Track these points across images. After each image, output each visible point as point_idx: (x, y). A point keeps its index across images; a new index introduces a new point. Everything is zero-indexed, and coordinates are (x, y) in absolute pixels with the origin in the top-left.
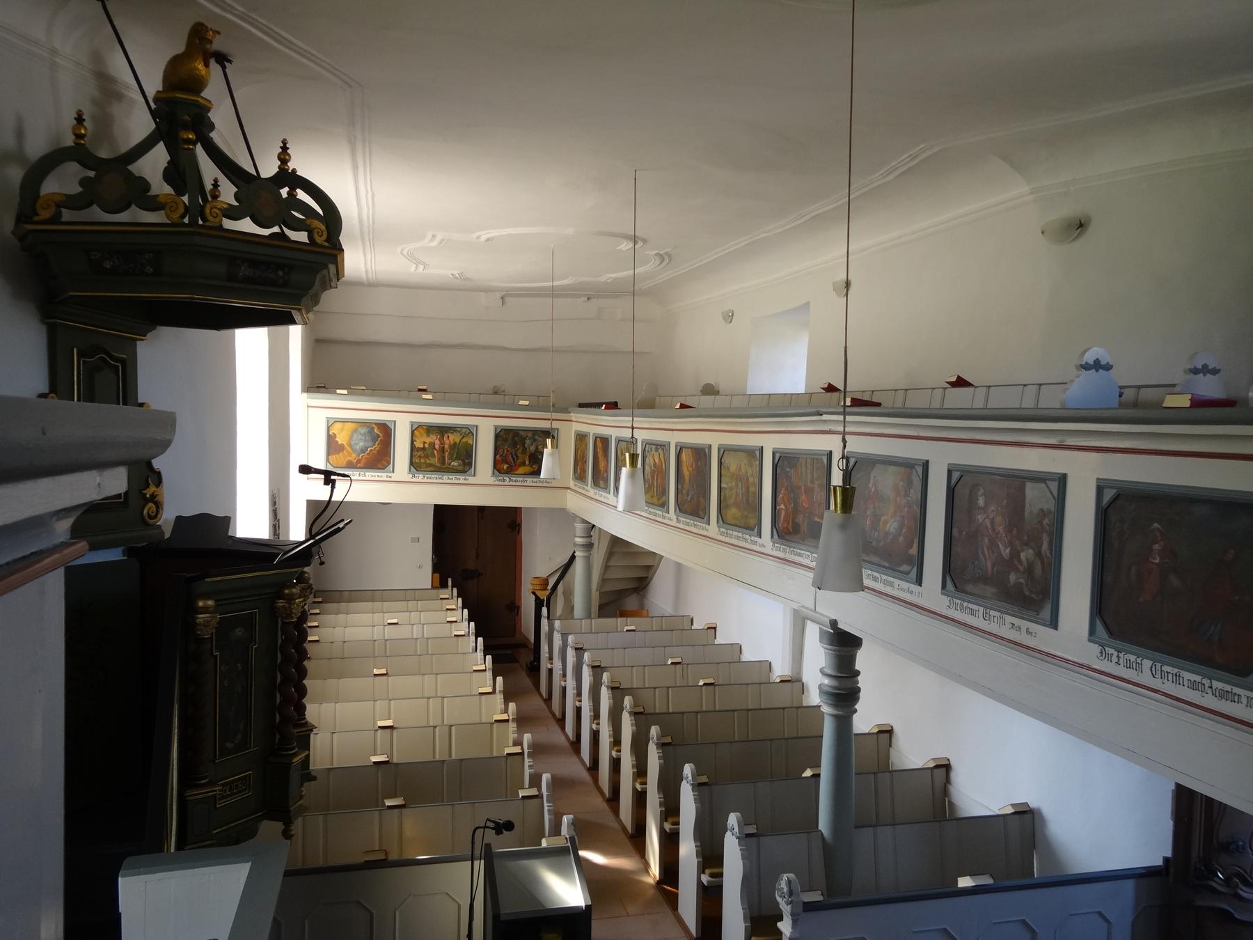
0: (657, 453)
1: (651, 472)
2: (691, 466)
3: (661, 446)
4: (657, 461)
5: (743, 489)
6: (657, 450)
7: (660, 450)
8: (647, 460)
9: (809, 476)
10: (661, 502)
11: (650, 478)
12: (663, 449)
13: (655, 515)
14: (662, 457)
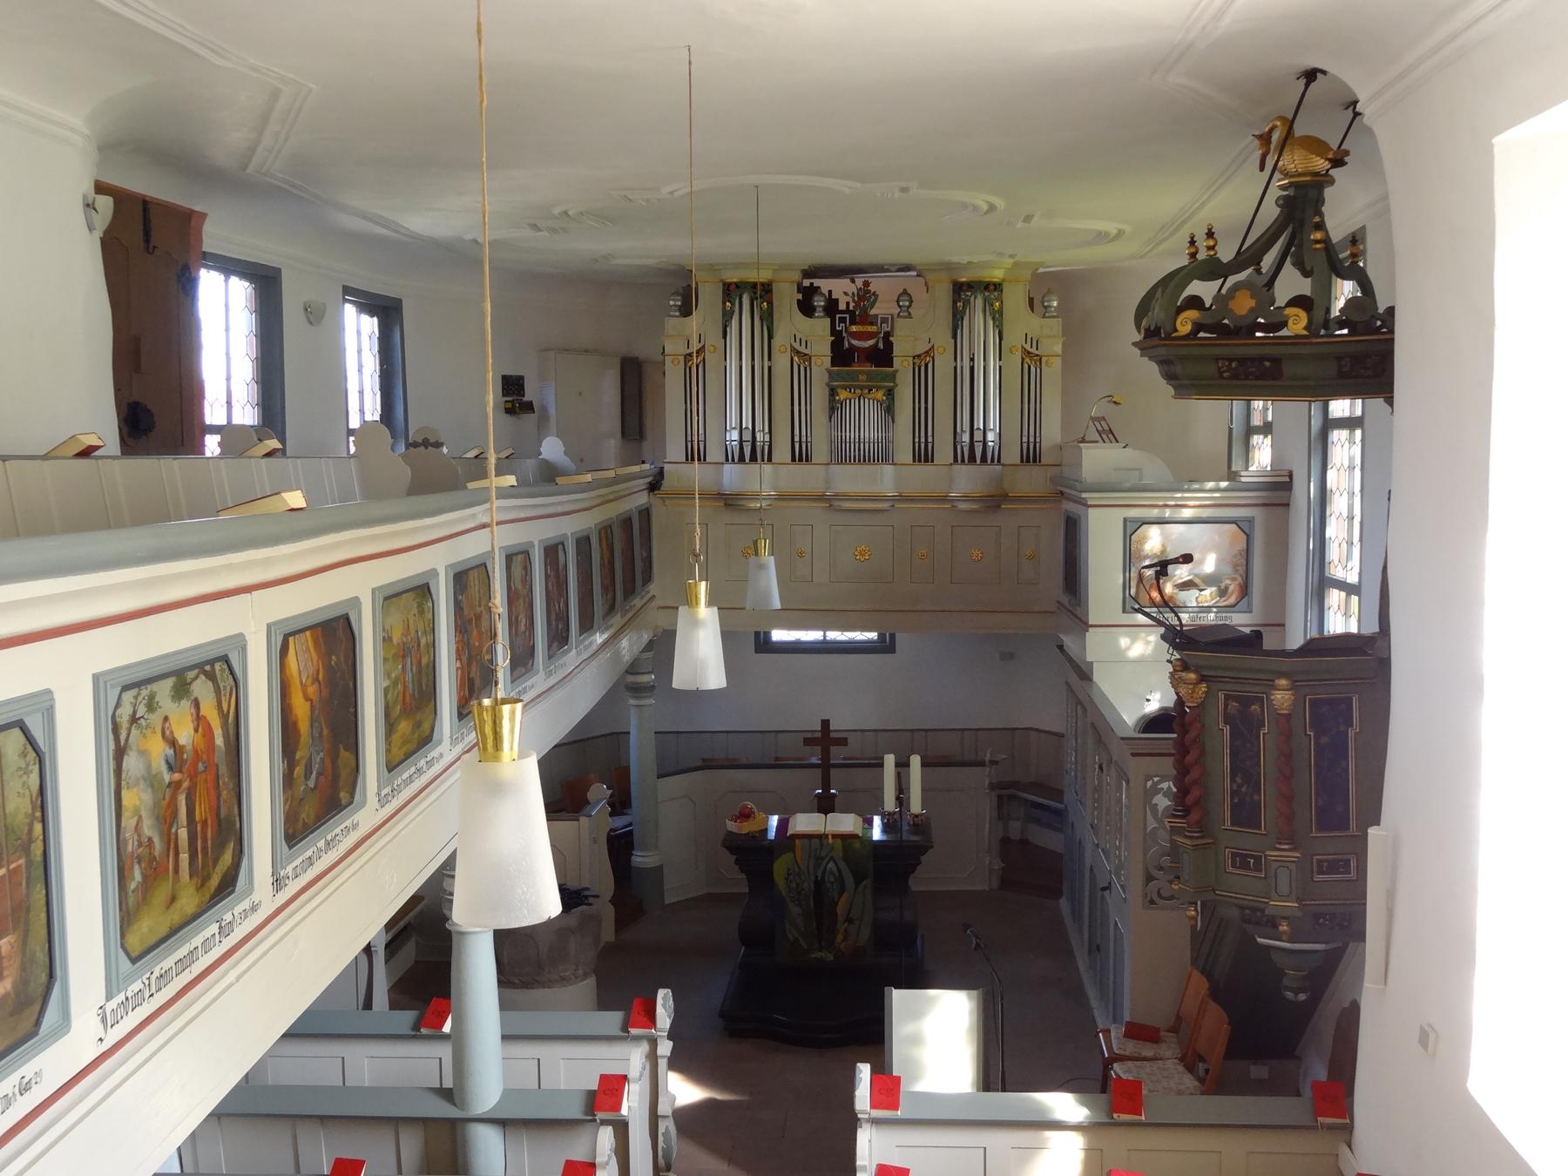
0: (186, 704)
1: (156, 805)
2: (316, 680)
3: (200, 666)
4: (185, 734)
5: (414, 670)
6: (181, 690)
7: (202, 688)
8: (131, 762)
9: (477, 595)
10: (215, 882)
11: (148, 829)
12: (211, 676)
13: (192, 957)
14: (209, 710)
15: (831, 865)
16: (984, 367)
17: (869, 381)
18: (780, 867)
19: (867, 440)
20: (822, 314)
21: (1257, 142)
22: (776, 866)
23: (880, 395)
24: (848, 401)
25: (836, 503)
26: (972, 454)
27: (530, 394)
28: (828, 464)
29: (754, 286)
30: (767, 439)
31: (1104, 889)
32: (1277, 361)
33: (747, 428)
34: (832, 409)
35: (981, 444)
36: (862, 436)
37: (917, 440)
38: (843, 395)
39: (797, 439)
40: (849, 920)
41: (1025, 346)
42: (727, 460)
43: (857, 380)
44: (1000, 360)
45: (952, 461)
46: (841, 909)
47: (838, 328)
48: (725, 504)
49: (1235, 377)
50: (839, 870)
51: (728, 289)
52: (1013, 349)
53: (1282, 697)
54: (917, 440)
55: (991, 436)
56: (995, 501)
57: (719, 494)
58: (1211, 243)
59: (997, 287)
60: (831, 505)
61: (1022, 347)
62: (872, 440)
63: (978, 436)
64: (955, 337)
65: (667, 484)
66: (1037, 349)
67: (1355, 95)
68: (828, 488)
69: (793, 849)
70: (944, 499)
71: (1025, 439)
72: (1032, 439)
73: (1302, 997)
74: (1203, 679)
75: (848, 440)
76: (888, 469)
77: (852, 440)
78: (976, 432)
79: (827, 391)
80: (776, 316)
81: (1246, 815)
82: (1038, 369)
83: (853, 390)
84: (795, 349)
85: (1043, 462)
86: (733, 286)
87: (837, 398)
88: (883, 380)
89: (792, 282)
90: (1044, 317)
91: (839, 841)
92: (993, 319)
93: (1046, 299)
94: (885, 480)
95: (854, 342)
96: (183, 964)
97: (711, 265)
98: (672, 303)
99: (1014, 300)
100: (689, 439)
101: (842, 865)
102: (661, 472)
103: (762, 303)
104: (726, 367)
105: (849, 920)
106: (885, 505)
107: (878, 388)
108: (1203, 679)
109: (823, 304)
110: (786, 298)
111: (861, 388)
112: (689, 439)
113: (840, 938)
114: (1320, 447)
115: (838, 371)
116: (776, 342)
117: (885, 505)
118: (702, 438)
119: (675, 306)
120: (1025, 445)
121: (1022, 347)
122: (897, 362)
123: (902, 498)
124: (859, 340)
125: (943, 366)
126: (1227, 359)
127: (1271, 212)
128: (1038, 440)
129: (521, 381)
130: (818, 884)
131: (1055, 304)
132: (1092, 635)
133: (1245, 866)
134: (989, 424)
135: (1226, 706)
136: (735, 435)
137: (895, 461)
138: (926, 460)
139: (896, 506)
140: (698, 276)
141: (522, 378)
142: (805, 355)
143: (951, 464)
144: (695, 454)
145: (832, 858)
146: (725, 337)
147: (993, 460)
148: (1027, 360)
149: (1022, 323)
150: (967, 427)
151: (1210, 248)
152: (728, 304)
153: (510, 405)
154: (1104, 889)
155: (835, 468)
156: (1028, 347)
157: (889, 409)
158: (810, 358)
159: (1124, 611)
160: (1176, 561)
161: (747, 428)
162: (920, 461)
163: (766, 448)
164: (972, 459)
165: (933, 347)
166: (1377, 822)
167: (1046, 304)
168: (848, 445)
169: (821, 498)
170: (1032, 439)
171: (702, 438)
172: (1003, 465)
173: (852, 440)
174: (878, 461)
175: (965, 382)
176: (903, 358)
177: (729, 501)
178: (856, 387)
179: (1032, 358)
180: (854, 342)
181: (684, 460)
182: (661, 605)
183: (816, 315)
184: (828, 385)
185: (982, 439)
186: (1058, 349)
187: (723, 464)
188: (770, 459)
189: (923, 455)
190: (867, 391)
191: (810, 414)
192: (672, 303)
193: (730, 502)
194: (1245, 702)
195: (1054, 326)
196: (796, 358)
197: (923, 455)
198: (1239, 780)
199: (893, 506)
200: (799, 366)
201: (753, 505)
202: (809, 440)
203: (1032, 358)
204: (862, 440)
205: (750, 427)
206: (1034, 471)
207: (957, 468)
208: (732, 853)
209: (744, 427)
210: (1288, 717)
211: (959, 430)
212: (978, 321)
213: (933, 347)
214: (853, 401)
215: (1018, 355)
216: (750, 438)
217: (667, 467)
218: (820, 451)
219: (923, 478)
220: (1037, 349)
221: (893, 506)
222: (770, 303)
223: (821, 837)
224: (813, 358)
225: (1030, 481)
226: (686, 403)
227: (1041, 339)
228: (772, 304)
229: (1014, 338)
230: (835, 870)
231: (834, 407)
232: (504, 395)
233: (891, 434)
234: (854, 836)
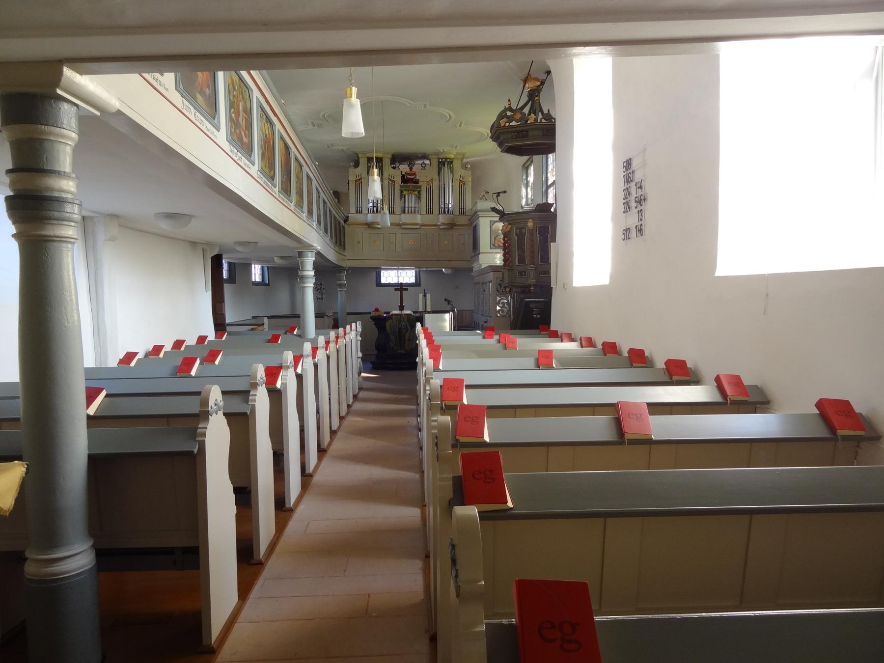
15: (403, 323)
18: (388, 324)
21: (522, 82)
22: (387, 324)
23: (416, 193)
25: (403, 227)
26: (445, 211)
31: (485, 322)
32: (527, 131)
34: (401, 197)
38: (405, 192)
39: (390, 207)
40: (409, 340)
43: (409, 188)
46: (407, 337)
49: (516, 138)
50: (406, 325)
53: (530, 224)
55: (450, 206)
56: (451, 226)
58: (510, 103)
63: (446, 206)
64: (439, 176)
65: (350, 220)
67: (549, 67)
69: (392, 319)
70: (436, 225)
71: (461, 208)
73: (538, 316)
74: (509, 224)
78: (446, 205)
81: (522, 260)
88: (417, 188)
90: (466, 170)
91: (406, 316)
92: (451, 170)
94: (418, 219)
95: (409, 177)
96: (268, 185)
97: (364, 152)
99: (457, 165)
101: (407, 324)
105: (409, 340)
106: (418, 227)
107: (416, 191)
108: (509, 224)
110: (387, 162)
111: (411, 191)
113: (406, 346)
114: (545, 195)
118: (361, 206)
122: (421, 184)
125: (435, 184)
126: (516, 132)
127: (525, 99)
130: (400, 329)
131: (469, 166)
132: (481, 256)
133: (522, 275)
135: (516, 231)
136: (371, 205)
140: (360, 156)
144: (359, 212)
145: (404, 321)
149: (459, 172)
150: (443, 203)
151: (509, 104)
154: (485, 322)
156: (461, 179)
157: (419, 197)
159: (490, 248)
160: (501, 192)
165: (432, 179)
166: (555, 241)
169: (398, 225)
171: (361, 206)
175: (442, 190)
177: (370, 225)
178: (408, 190)
179: (462, 183)
180: (409, 177)
182: (348, 258)
186: (470, 180)
189: (430, 212)
191: (394, 199)
194: (521, 229)
195: (469, 172)
197: (430, 212)
198: (520, 251)
201: (377, 226)
203: (462, 183)
206: (464, 216)
208: (373, 321)
210: (532, 230)
212: (446, 169)
213: (432, 179)
216: (376, 205)
218: (398, 210)
219: (429, 219)
222: (382, 164)
223: (400, 315)
225: (463, 220)
229: (457, 176)
230: (405, 325)
231: (402, 196)
234: (411, 315)
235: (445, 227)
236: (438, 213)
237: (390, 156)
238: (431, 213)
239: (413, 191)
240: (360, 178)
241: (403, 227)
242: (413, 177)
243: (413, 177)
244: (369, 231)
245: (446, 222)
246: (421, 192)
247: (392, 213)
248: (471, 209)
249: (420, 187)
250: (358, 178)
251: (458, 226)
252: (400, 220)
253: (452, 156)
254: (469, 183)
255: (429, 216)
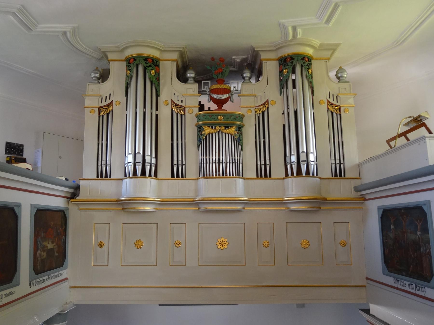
16: (304, 111)
17: (225, 120)
19: (224, 161)
20: (193, 82)
24: (211, 135)
25: (203, 207)
27: (26, 154)
28: (197, 179)
29: (146, 59)
30: (154, 161)
33: (139, 153)
34: (200, 141)
35: (306, 162)
36: (221, 159)
37: (259, 163)
38: (207, 130)
39: (175, 162)
41: (329, 99)
42: (126, 176)
43: (218, 120)
44: (313, 109)
45: (284, 176)
47: (203, 89)
48: (123, 209)
51: (129, 63)
52: (321, 102)
54: (259, 163)
55: (312, 157)
57: (117, 201)
59: (310, 59)
60: (199, 208)
61: (328, 100)
62: (228, 161)
63: (303, 157)
64: (281, 95)
65: (83, 194)
66: (337, 102)
68: (197, 196)
70: (281, 203)
71: (333, 162)
72: (338, 162)
75: (211, 162)
76: (240, 181)
77: (214, 161)
78: (301, 155)
79: (196, 129)
80: (162, 82)
82: (339, 116)
83: (214, 127)
84: (174, 103)
85: (347, 176)
86: (132, 60)
87: (203, 133)
88: (235, 119)
89: (173, 61)
93: (339, 72)
98: (93, 75)
100: (100, 163)
102: (77, 188)
103: (152, 70)
104: (127, 115)
106: (239, 207)
107: (231, 126)
109: (193, 75)
112: (100, 163)
115: (204, 114)
116: (162, 99)
117: (239, 207)
119: (95, 77)
120: (333, 166)
121: (328, 100)
123: (250, 203)
124: (218, 93)
128: (342, 162)
129: (21, 148)
134: (310, 149)
136: (130, 158)
137: (244, 176)
138: (266, 176)
139: (246, 208)
141: (22, 146)
142: (181, 107)
143: (284, 179)
146: (127, 95)
147: (313, 175)
148: (331, 109)
152: (128, 72)
153: (9, 159)
155: (202, 181)
156: (331, 100)
157: (239, 141)
158: (185, 108)
161: (139, 153)
162: (261, 176)
163: (153, 168)
164: (299, 172)
165: (268, 101)
167: (339, 75)
168: (211, 165)
170: (338, 162)
171: (108, 163)
172: (321, 178)
173: (214, 161)
174: (233, 175)
176: (248, 108)
181: (95, 177)
182: (73, 285)
183: (189, 82)
184: (197, 125)
185: (306, 160)
187: (122, 180)
188: (156, 175)
190: (224, 128)
192: (93, 75)
193: (125, 207)
196: (174, 109)
199: (244, 208)
200: (177, 114)
202: (184, 163)
204: (221, 161)
205: (141, 152)
207: (290, 180)
209: (137, 152)
211: (288, 154)
213: (268, 101)
214: (214, 135)
215: (325, 106)
217: (82, 183)
220: (337, 102)
221: (244, 208)
222: (158, 74)
224: (187, 109)
226: (99, 139)
227: (341, 96)
228: (159, 74)
232: (6, 153)
233: (241, 158)
235: (303, 207)
236: (284, 176)
237: (175, 56)
238: (266, 176)
239: (227, 127)
240: (108, 101)
241: (203, 207)
242: (225, 96)
243: (225, 96)
244: (126, 218)
245: (306, 195)
246: (243, 129)
247: (178, 176)
248: (359, 166)
249: (241, 118)
250: (104, 104)
251: (335, 202)
252: (197, 191)
253: (309, 51)
254: (349, 109)
255: (264, 182)
